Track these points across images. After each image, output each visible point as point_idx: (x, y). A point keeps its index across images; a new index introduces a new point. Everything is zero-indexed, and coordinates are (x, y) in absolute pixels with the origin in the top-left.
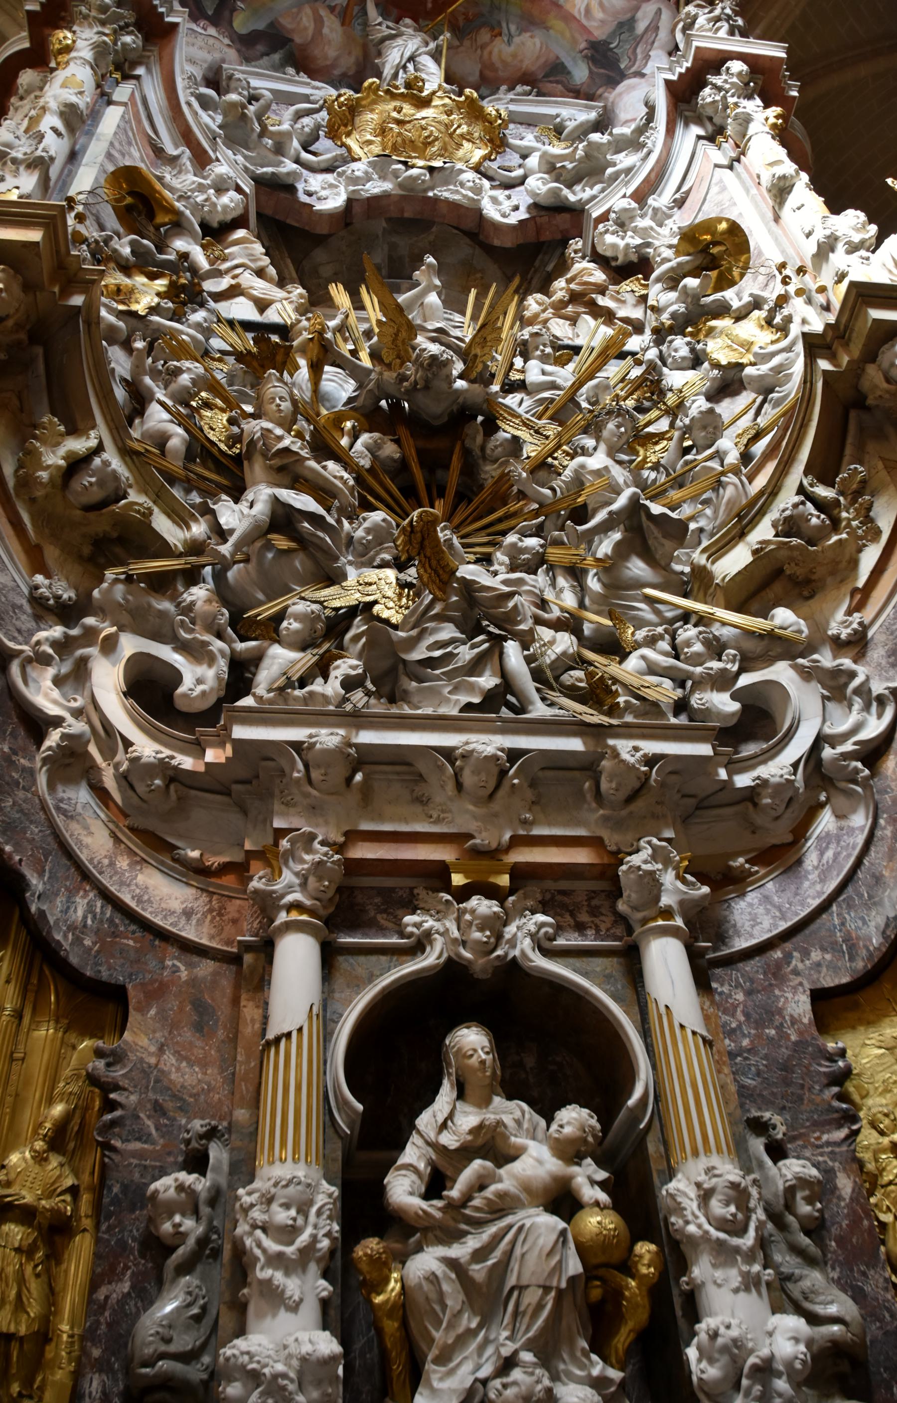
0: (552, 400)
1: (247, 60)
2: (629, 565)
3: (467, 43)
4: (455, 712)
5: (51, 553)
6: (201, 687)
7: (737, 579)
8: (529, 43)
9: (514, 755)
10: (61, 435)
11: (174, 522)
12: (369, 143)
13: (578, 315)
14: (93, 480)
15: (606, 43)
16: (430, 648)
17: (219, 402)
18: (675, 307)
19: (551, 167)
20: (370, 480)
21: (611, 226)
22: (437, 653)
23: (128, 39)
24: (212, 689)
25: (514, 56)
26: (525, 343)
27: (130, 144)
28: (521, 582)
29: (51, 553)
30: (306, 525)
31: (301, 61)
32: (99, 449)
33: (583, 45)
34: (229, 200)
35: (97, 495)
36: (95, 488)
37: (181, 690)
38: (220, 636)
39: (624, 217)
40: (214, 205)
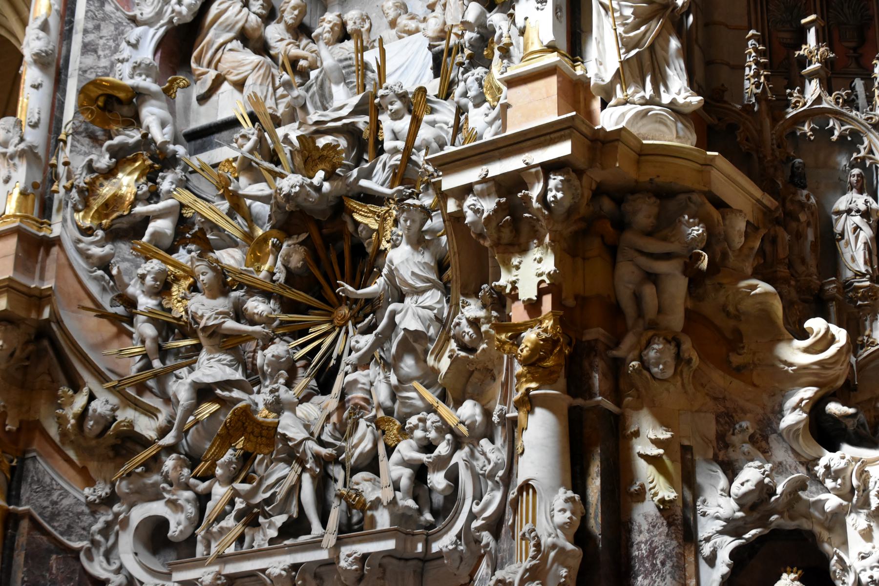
4: (266, 546)
5: (92, 466)
6: (181, 527)
9: (295, 567)
10: (72, 396)
11: (149, 417)
16: (265, 492)
22: (268, 495)
24: (185, 528)
28: (355, 382)
29: (92, 466)
32: (92, 397)
35: (98, 429)
36: (95, 427)
37: (170, 534)
38: (187, 487)
40: (180, 13)
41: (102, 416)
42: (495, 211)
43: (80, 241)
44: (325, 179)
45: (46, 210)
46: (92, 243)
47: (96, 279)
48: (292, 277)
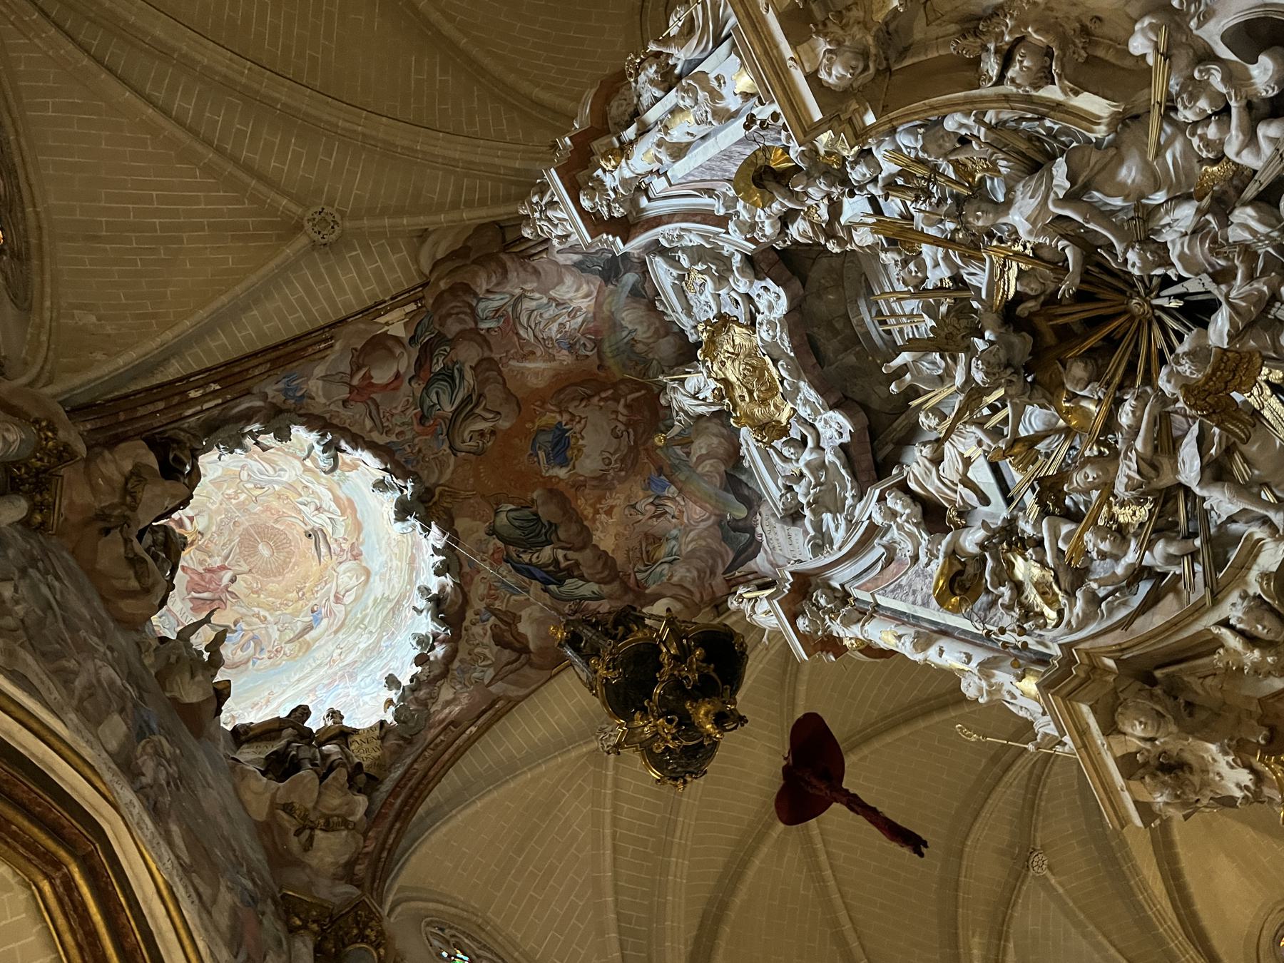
0: (962, 256)
1: (760, 497)
2: (1129, 181)
3: (651, 356)
7: (1109, 94)
8: (628, 319)
10: (1227, 650)
11: (1259, 551)
12: (776, 406)
13: (842, 227)
14: (1260, 627)
15: (600, 274)
17: (1105, 509)
18: (823, 186)
19: (722, 279)
20: (1117, 380)
21: (757, 235)
23: (822, 602)
25: (641, 323)
26: (916, 287)
27: (900, 586)
30: (1213, 451)
31: (734, 457)
32: (1225, 623)
33: (611, 287)
34: (895, 502)
39: (746, 229)
41: (1248, 611)
42: (825, 36)
43: (1069, 622)
44: (982, 337)
45: (1043, 660)
46: (1071, 611)
47: (1111, 611)
48: (1096, 377)
